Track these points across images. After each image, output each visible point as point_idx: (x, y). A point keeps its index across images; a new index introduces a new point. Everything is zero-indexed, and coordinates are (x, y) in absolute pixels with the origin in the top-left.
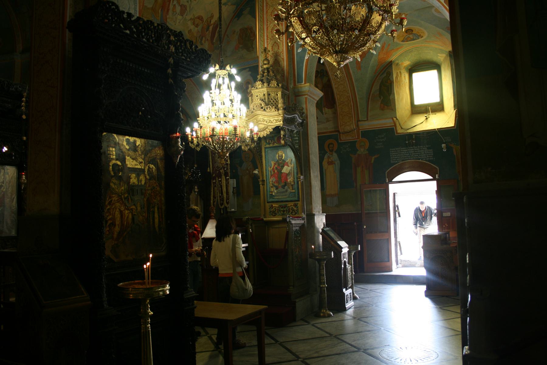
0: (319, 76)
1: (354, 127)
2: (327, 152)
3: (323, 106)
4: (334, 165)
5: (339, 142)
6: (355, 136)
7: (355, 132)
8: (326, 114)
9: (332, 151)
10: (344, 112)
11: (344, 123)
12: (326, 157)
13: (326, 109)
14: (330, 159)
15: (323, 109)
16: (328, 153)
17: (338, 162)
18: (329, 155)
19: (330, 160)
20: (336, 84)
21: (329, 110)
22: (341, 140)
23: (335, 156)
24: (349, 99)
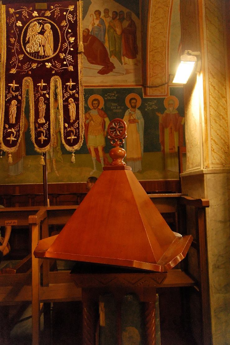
0: (118, 18)
1: (166, 80)
2: (129, 108)
3: (122, 55)
4: (137, 124)
5: (144, 97)
6: (165, 92)
7: (165, 88)
8: (126, 64)
9: (134, 107)
10: (156, 60)
11: (154, 74)
12: (127, 113)
13: (126, 59)
14: (132, 117)
15: (122, 58)
16: (129, 110)
17: (141, 121)
18: (130, 111)
19: (132, 118)
20: (153, 21)
21: (130, 60)
22: (146, 94)
23: (138, 112)
24: (165, 45)
